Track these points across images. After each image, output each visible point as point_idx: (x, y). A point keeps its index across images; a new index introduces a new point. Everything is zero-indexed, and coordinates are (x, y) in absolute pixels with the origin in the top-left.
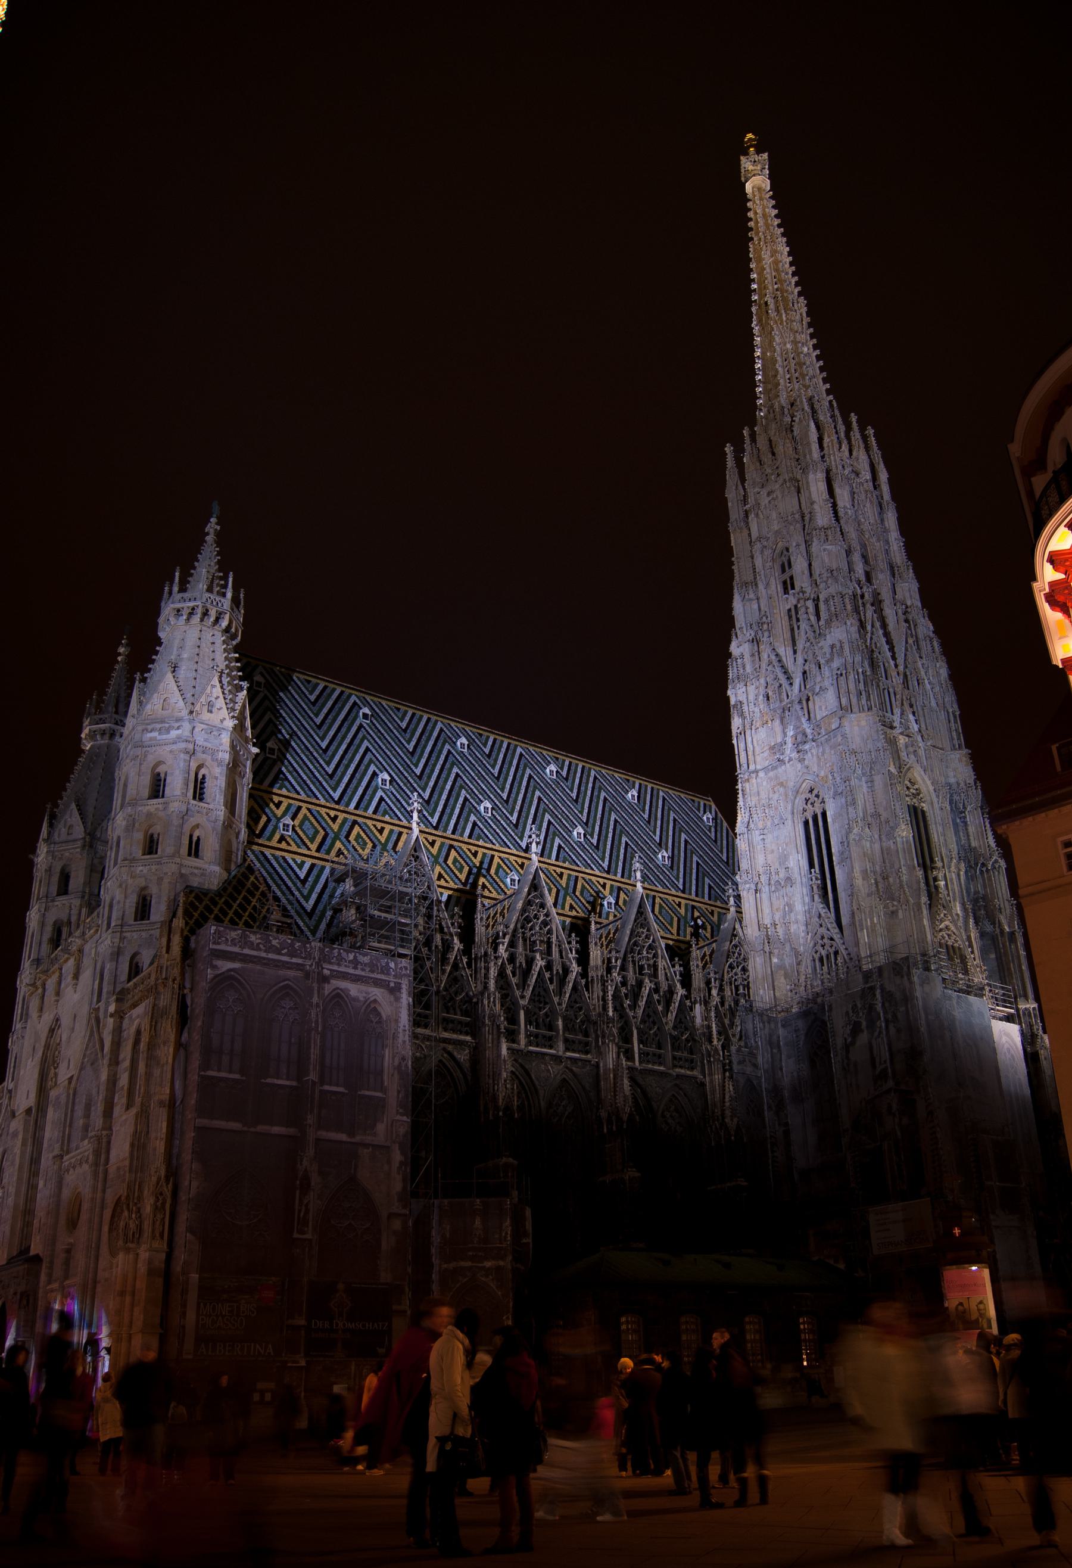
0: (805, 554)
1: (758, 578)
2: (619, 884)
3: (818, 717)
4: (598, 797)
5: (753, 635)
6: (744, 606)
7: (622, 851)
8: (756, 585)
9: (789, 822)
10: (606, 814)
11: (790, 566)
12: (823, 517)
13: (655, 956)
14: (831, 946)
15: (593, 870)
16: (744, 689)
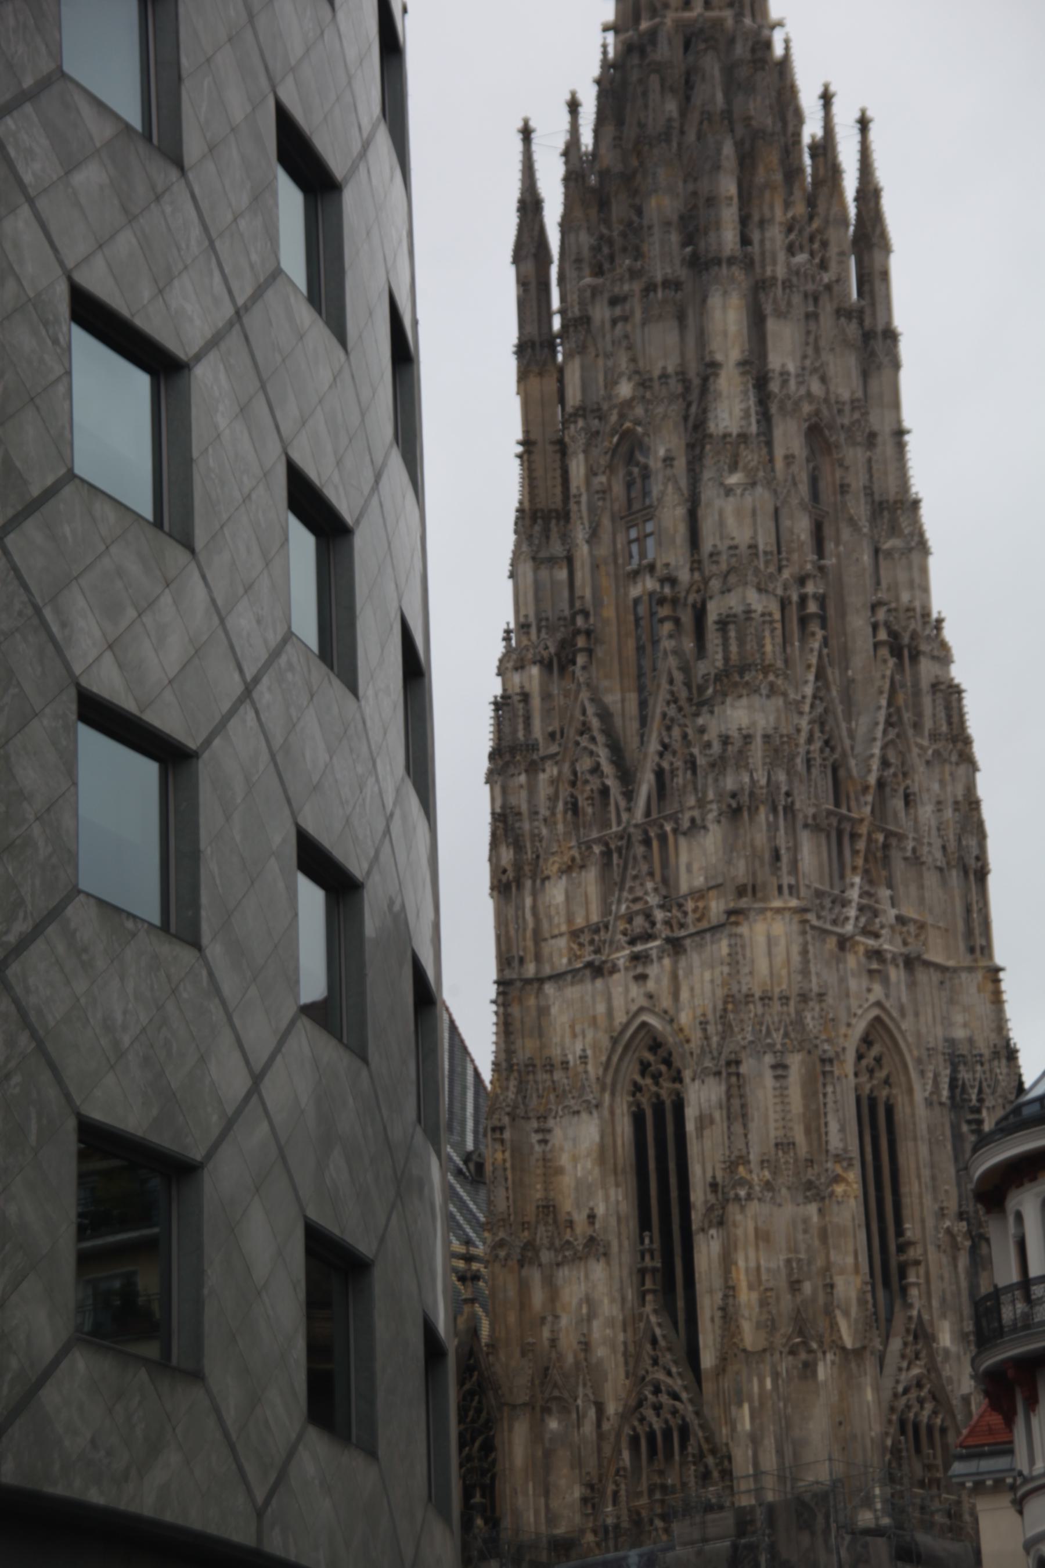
0: (683, 483)
1: (573, 507)
3: (684, 888)
5: (552, 650)
6: (536, 570)
8: (564, 516)
16: (523, 778)
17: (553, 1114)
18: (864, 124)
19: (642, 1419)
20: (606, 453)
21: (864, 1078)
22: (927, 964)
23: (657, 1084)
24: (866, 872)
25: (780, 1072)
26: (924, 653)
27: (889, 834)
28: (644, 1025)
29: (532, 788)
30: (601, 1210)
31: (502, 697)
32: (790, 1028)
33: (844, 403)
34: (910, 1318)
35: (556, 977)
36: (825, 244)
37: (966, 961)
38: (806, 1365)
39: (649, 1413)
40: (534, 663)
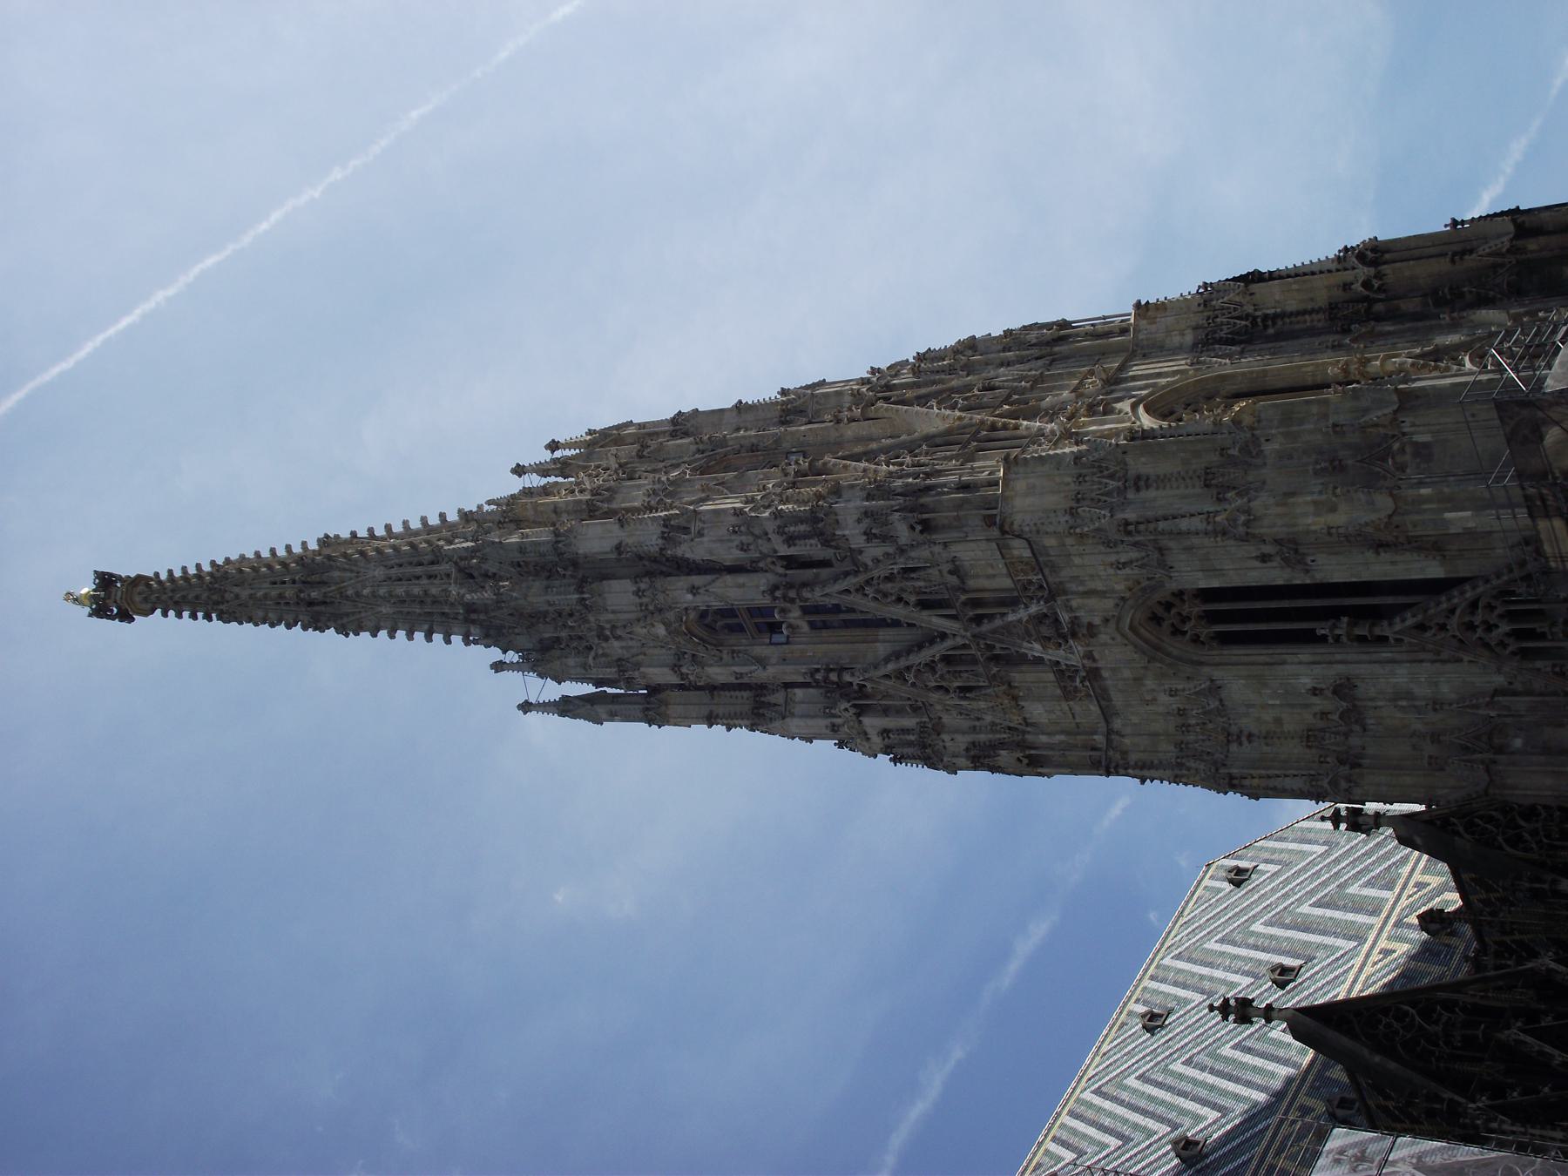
0: (709, 578)
1: (745, 680)
3: (1007, 583)
4: (1135, 1091)
5: (847, 705)
6: (793, 715)
7: (1248, 1059)
8: (760, 689)
9: (1217, 674)
10: (1169, 1081)
11: (730, 612)
12: (647, 536)
13: (1449, 1006)
14: (1490, 608)
15: (1267, 1128)
16: (945, 737)
18: (553, 446)
19: (1502, 644)
20: (707, 649)
22: (1122, 368)
23: (1189, 618)
25: (1142, 483)
26: (888, 382)
28: (1131, 628)
29: (957, 731)
30: (1306, 682)
34: (1413, 365)
35: (1107, 714)
39: (1496, 635)
40: (860, 722)
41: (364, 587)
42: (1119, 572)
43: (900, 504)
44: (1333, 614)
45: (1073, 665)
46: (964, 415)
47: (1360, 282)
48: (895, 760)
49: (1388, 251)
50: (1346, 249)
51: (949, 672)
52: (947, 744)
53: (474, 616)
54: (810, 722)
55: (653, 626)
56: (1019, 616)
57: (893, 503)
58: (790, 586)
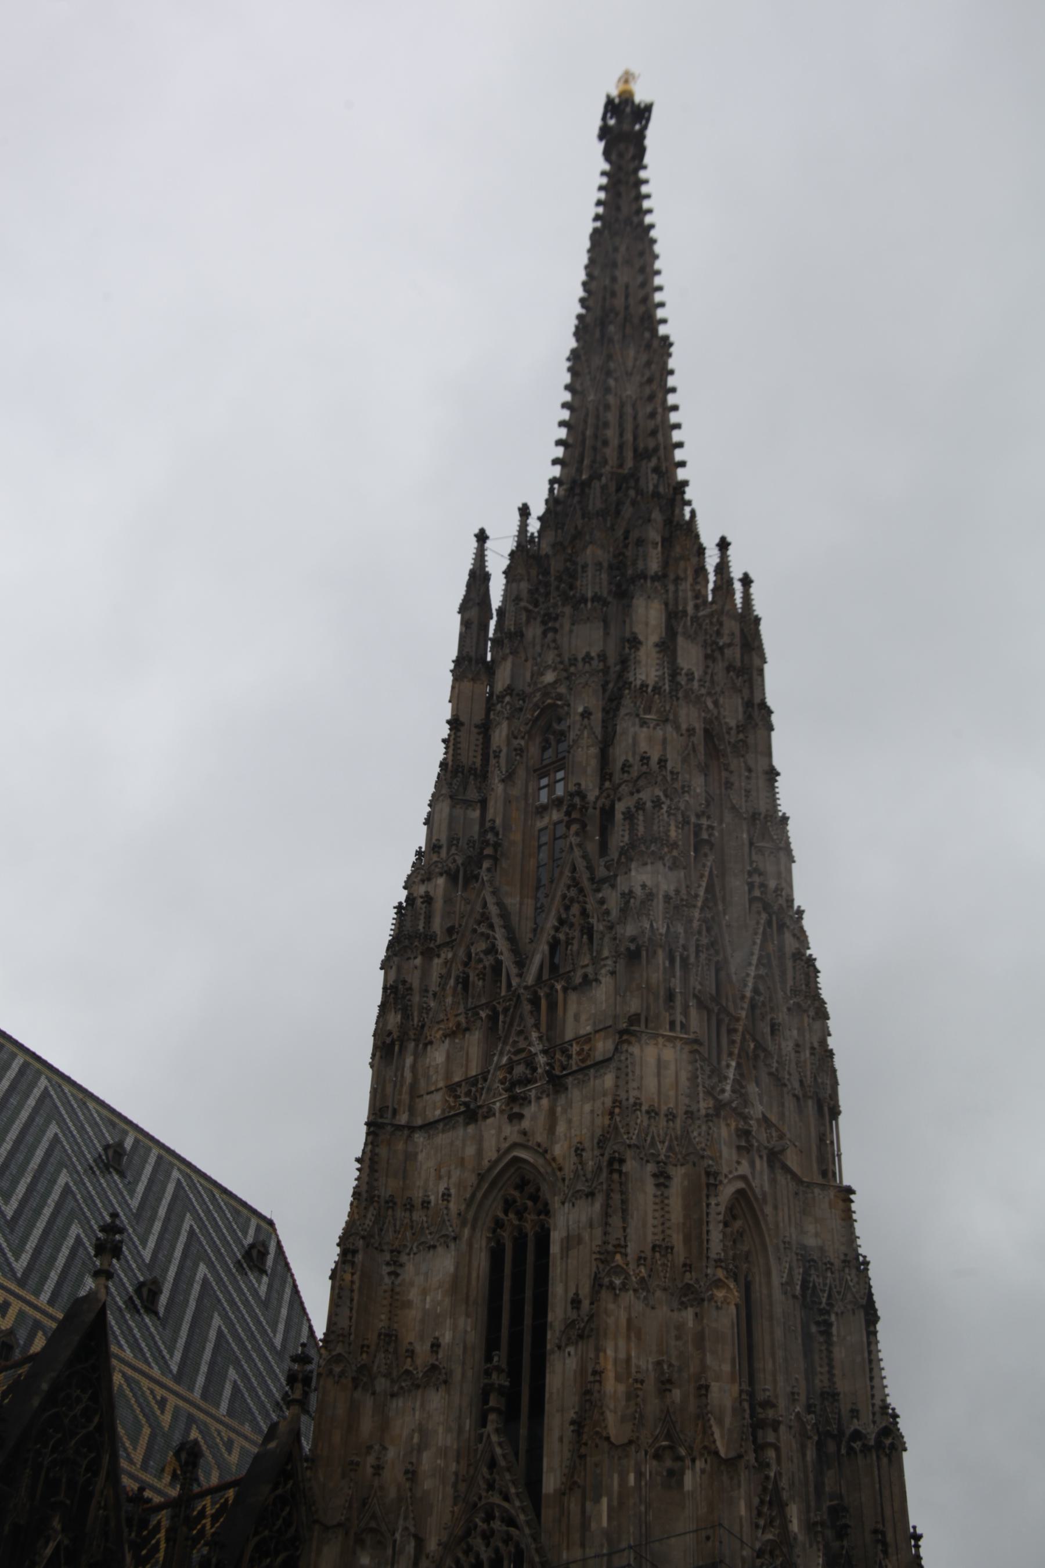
0: (598, 730)
1: (493, 761)
2: (38, 1316)
3: (569, 1035)
4: (43, 1132)
5: (459, 861)
6: (453, 807)
7: (65, 1251)
8: (483, 776)
10: (50, 1168)
16: (418, 961)
17: (408, 1250)
18: (746, 581)
20: (527, 724)
21: (730, 1244)
22: (787, 1169)
24: (739, 1065)
25: (662, 1180)
26: (788, 927)
27: (759, 1046)
28: (516, 1160)
30: (447, 1338)
31: (408, 899)
32: (675, 1143)
33: (731, 729)
34: (767, 1478)
35: (428, 1127)
36: (721, 624)
37: (820, 1180)
38: (671, 1473)
39: (478, 1543)
40: (441, 874)
41: (616, 380)
42: (573, 1149)
43: (658, 929)
44: (514, 1371)
45: (481, 1094)
46: (747, 1000)
47: (860, 1428)
48: (399, 907)
49: (890, 1461)
50: (895, 1416)
51: (485, 968)
52: (411, 961)
53: (577, 491)
54: (444, 826)
55: (555, 669)
56: (536, 1043)
57: (660, 922)
58: (584, 808)
